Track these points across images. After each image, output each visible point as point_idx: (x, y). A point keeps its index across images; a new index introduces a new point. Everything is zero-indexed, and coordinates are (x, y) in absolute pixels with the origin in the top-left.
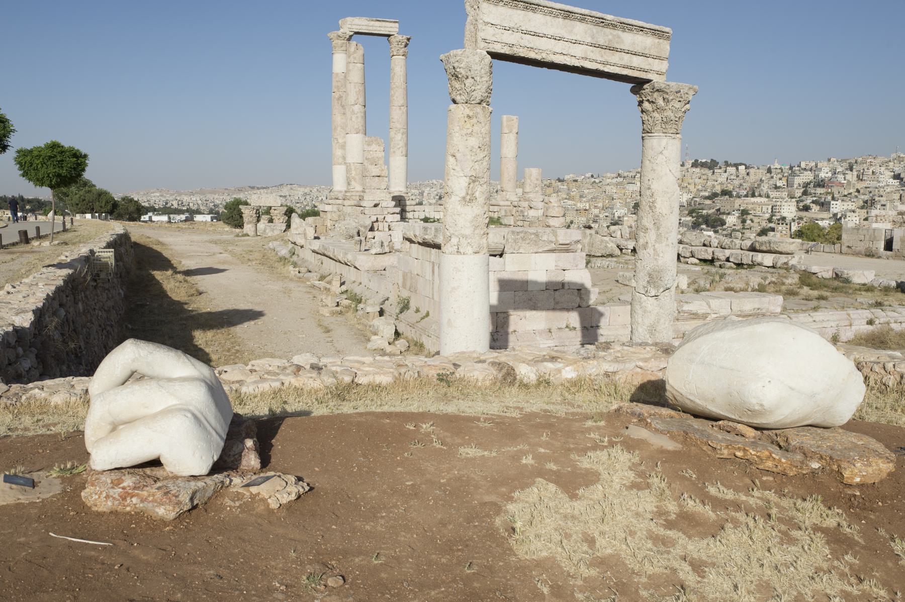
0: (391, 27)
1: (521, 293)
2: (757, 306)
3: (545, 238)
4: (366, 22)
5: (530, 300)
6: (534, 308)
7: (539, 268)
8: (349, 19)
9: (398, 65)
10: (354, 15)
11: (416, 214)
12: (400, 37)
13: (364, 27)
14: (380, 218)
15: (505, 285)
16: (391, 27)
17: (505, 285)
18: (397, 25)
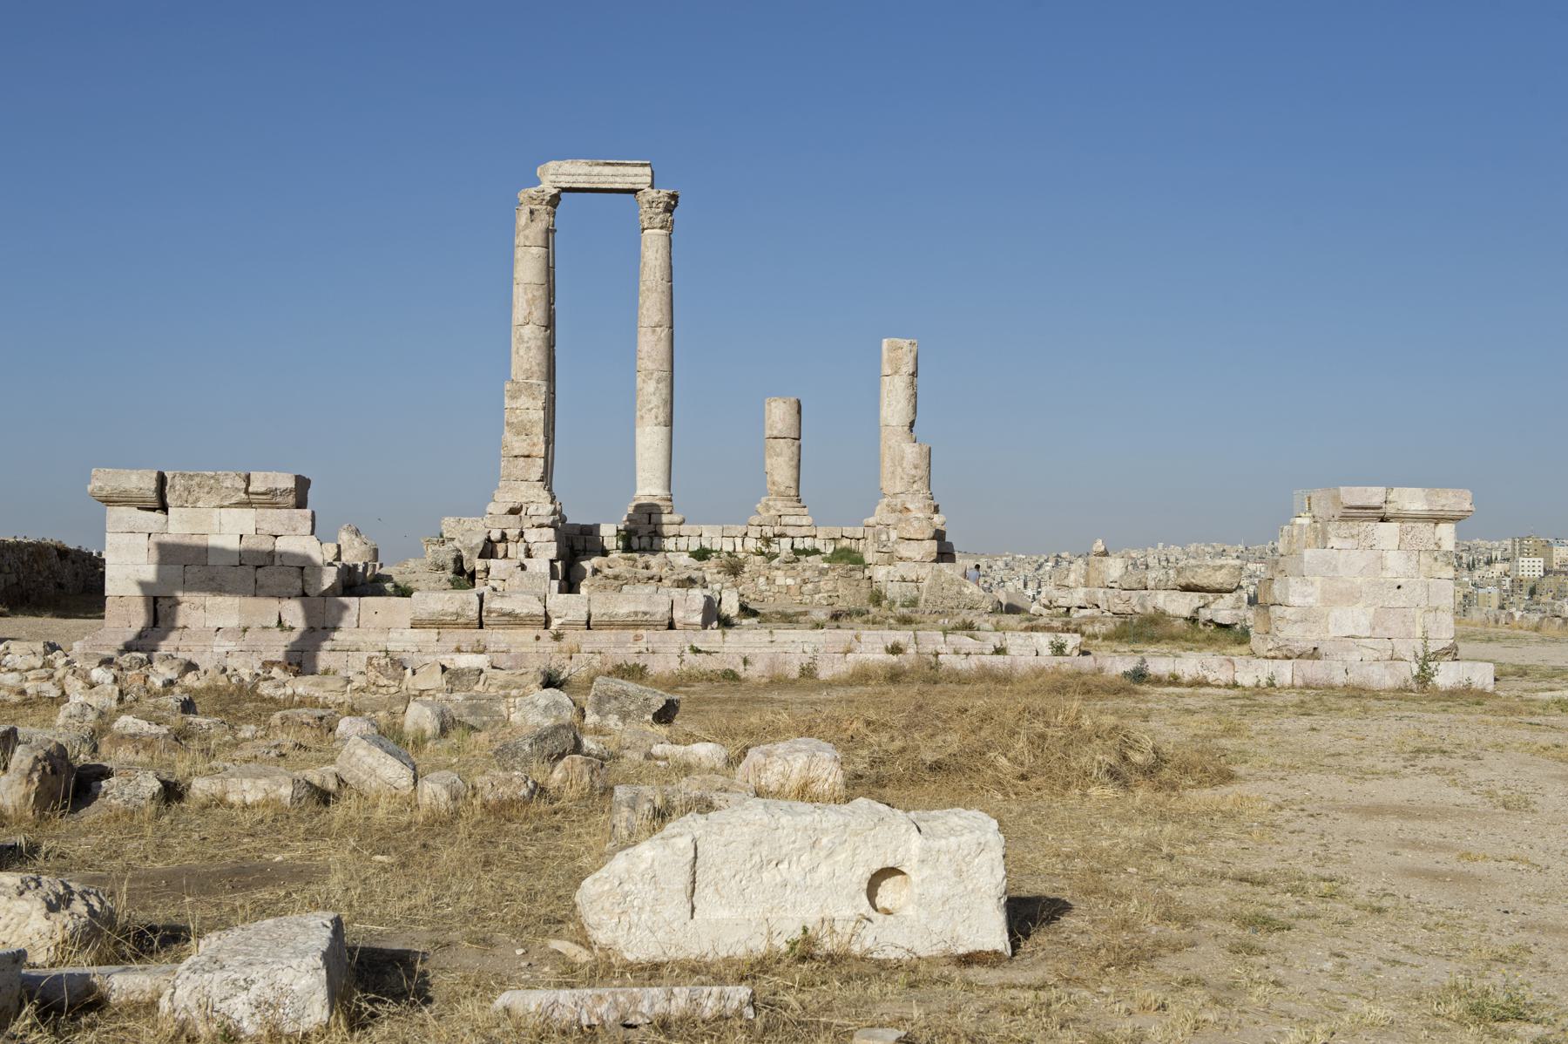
0: (637, 176)
1: (195, 569)
2: (643, 608)
3: (228, 483)
4: (587, 169)
5: (213, 579)
6: (219, 589)
7: (229, 529)
8: (552, 165)
9: (653, 245)
10: (562, 157)
11: (682, 543)
12: (653, 193)
13: (581, 179)
14: (512, 533)
15: (169, 554)
16: (637, 176)
17: (169, 554)
18: (648, 170)
